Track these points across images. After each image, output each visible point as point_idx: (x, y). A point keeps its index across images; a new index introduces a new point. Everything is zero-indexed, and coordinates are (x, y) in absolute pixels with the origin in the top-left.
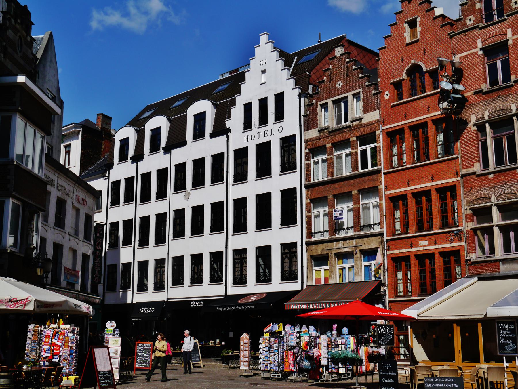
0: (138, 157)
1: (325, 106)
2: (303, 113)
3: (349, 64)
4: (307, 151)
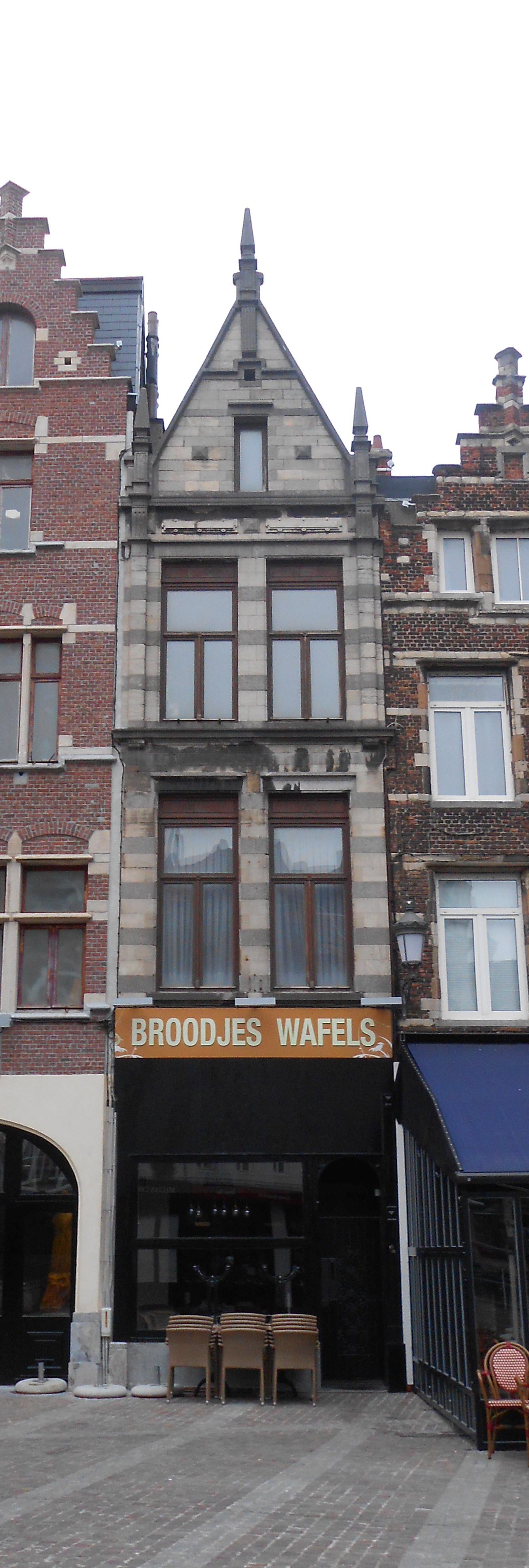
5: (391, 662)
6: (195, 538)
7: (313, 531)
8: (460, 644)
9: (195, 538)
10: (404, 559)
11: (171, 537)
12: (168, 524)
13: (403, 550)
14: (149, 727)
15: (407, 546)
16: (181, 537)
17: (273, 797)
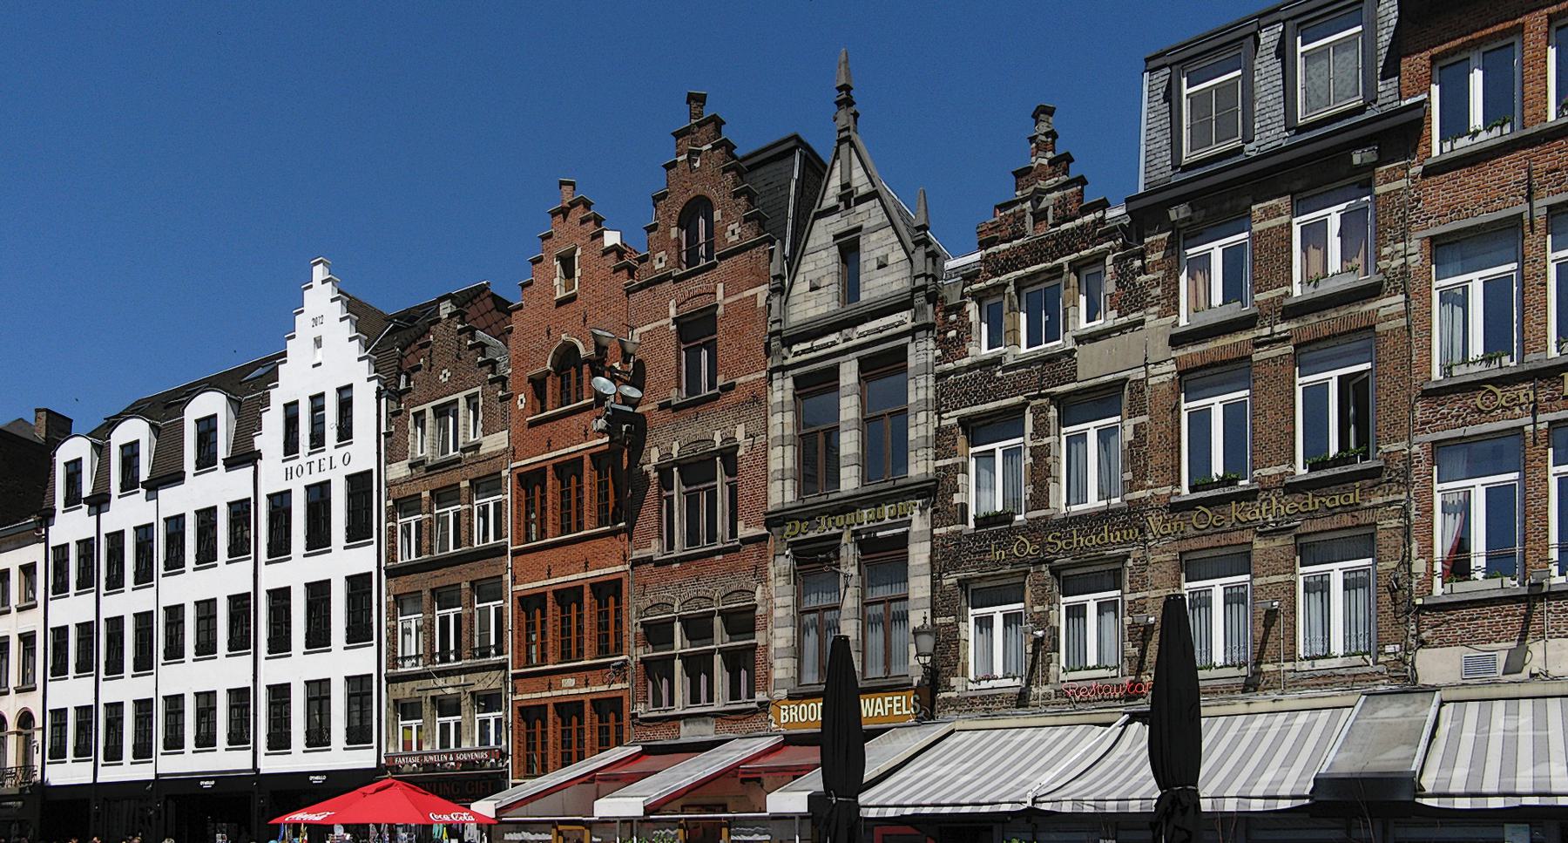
0: (99, 502)
1: (419, 418)
3: (462, 336)
4: (390, 503)
5: (939, 423)
6: (813, 355)
7: (887, 327)
9: (813, 355)
10: (952, 334)
11: (798, 359)
12: (795, 348)
13: (952, 326)
14: (787, 506)
15: (955, 321)
16: (804, 357)
17: (861, 545)
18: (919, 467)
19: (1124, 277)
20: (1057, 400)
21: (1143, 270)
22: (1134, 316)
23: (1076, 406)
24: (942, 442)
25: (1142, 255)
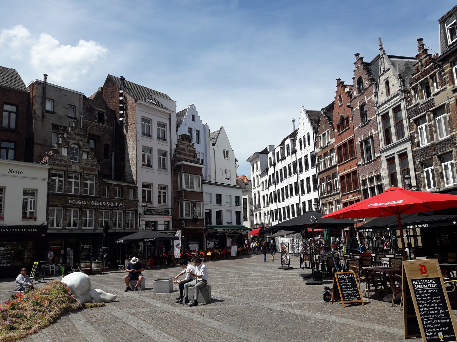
0: (274, 165)
2: (315, 141)
4: (317, 158)
8: (419, 113)
12: (380, 108)
18: (407, 134)
19: (441, 77)
20: (433, 112)
21: (444, 75)
22: (444, 87)
23: (436, 112)
24: (410, 127)
25: (443, 71)
